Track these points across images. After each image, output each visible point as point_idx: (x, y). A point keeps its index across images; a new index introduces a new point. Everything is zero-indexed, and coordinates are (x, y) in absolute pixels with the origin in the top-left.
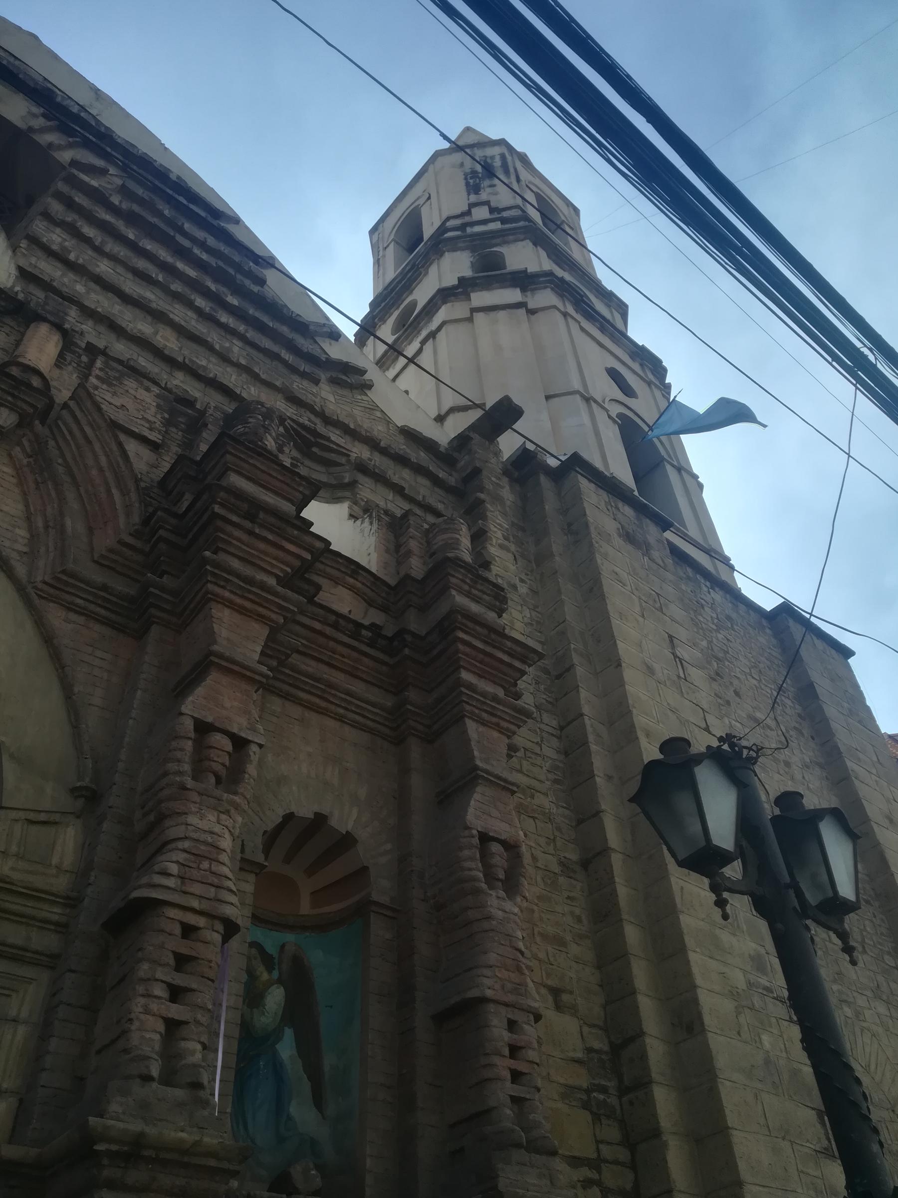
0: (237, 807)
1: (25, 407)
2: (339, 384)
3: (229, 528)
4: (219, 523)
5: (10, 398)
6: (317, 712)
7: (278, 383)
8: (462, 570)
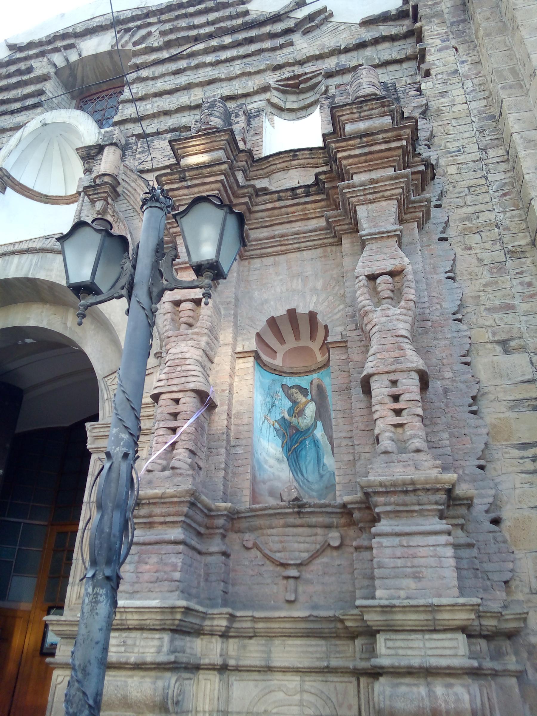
0: (198, 334)
1: (103, 195)
2: (309, 32)
3: (176, 193)
4: (170, 194)
5: (96, 196)
6: (284, 254)
7: (262, 67)
8: (347, 107)
